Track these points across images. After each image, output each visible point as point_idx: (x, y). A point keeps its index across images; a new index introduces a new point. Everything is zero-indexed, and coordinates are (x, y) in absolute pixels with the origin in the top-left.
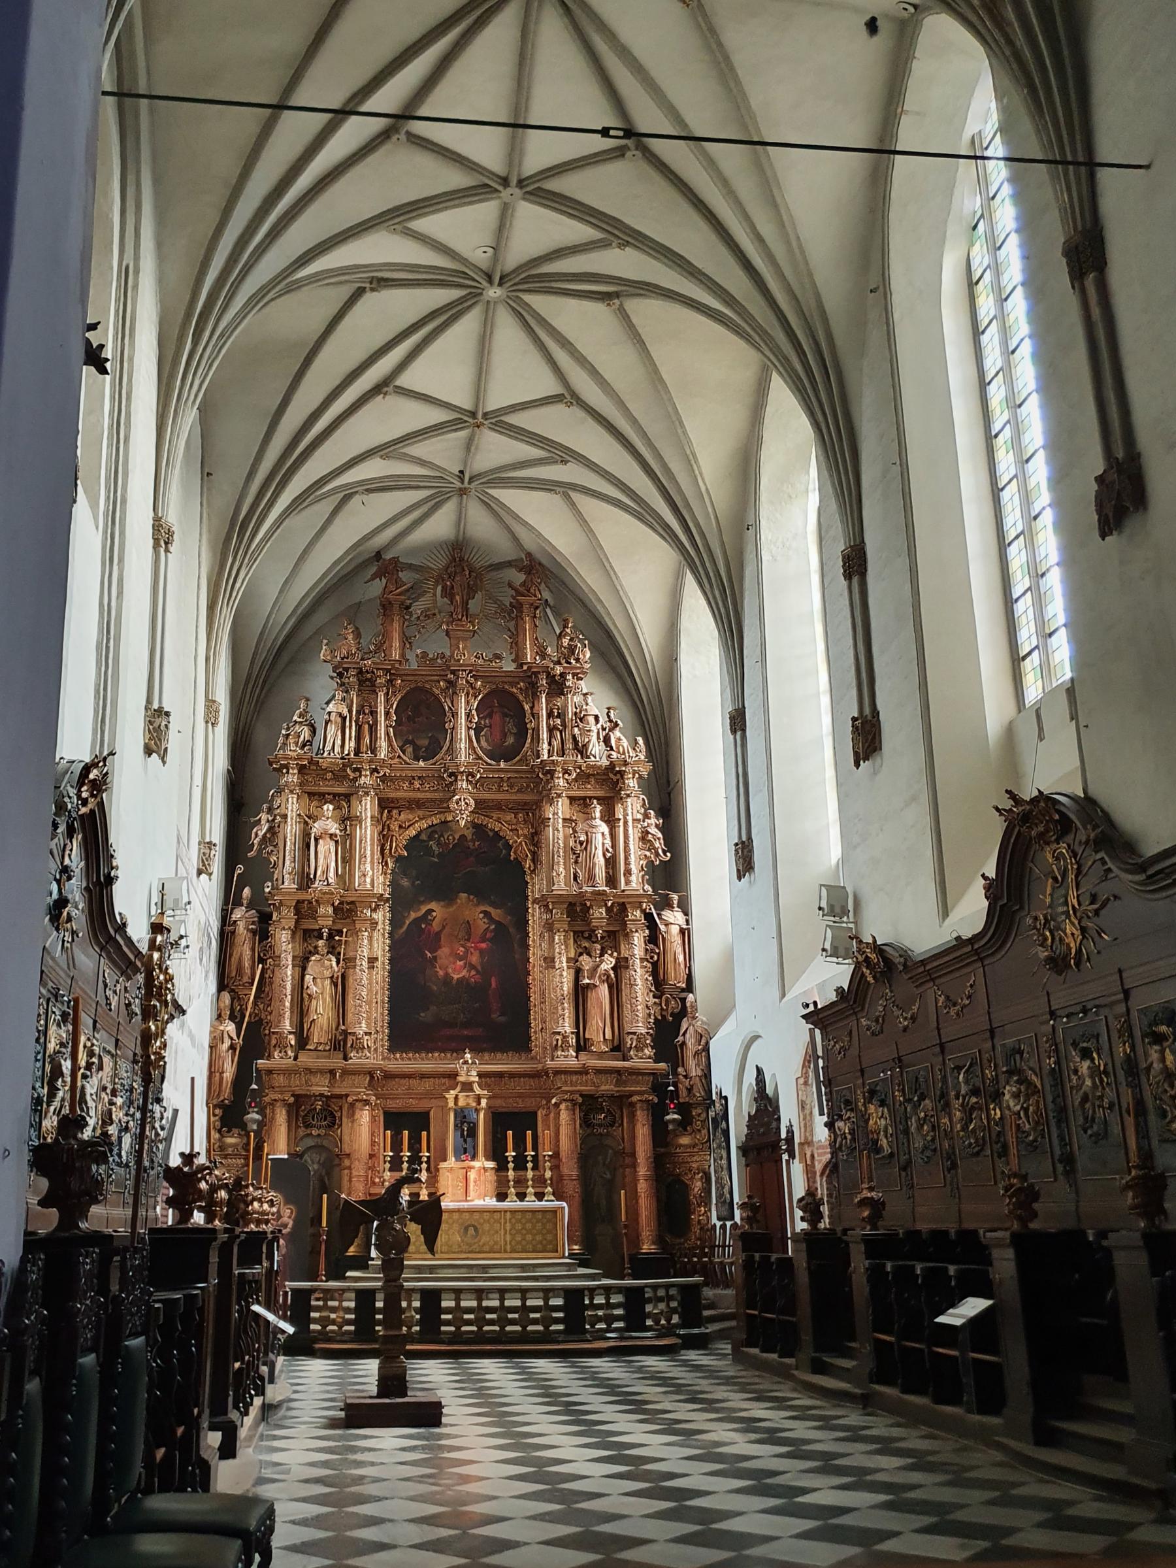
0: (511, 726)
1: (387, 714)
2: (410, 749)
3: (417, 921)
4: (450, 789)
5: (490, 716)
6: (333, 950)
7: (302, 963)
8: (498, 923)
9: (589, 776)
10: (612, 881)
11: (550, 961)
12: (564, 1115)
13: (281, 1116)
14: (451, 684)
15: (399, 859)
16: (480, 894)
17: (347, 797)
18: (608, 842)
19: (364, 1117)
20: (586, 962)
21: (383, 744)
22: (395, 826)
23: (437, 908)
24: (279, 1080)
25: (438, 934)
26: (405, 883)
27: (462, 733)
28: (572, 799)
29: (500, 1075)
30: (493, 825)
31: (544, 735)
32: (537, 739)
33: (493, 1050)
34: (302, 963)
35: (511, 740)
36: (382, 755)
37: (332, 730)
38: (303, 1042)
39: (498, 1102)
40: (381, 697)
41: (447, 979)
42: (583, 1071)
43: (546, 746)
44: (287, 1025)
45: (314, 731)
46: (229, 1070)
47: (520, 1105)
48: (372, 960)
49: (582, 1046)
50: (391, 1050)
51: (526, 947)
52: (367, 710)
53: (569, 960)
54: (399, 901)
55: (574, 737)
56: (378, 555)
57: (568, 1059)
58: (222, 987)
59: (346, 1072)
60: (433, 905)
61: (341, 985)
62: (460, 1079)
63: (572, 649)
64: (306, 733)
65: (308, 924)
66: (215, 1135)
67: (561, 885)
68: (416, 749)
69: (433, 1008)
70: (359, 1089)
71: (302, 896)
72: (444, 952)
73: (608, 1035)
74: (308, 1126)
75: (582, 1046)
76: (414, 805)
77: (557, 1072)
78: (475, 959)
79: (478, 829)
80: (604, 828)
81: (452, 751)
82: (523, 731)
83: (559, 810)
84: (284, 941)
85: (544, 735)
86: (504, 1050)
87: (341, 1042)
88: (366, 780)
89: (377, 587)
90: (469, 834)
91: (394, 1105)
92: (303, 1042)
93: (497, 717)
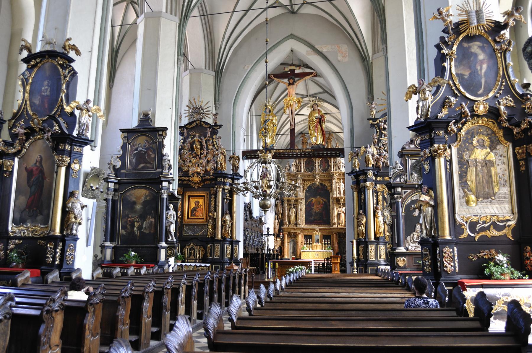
0: (326, 165)
1: (303, 164)
2: (308, 170)
3: (310, 202)
4: (314, 177)
5: (323, 163)
6: (294, 207)
7: (289, 210)
9: (340, 174)
11: (333, 209)
12: (335, 236)
13: (286, 236)
15: (306, 190)
16: (321, 196)
17: (296, 180)
19: (300, 236)
20: (340, 209)
21: (303, 170)
22: (305, 184)
23: (314, 199)
24: (286, 230)
25: (314, 204)
26: (308, 194)
27: (317, 167)
28: (338, 179)
29: (324, 229)
30: (324, 183)
31: (332, 166)
32: (331, 167)
33: (323, 224)
34: (289, 210)
35: (326, 167)
36: (302, 172)
37: (293, 167)
38: (290, 223)
39: (324, 234)
40: (302, 161)
41: (315, 212)
42: (338, 228)
43: (332, 169)
44: (287, 221)
45: (290, 168)
46: (277, 228)
47: (327, 234)
48: (301, 209)
49: (339, 224)
50: (306, 224)
51: (330, 206)
52: (300, 163)
53: (336, 209)
54: (307, 198)
55: (338, 167)
56: (302, 132)
57: (335, 226)
58: (276, 214)
59: (296, 229)
60: (313, 198)
61: (296, 213)
62: (316, 230)
64: (289, 168)
65: (290, 203)
66: (275, 239)
67: (335, 196)
68: (309, 170)
69: (313, 217)
70: (298, 232)
71: (289, 198)
72: (315, 207)
73: (343, 222)
74: (291, 237)
75: (339, 224)
76: (308, 180)
77: (333, 229)
78: (320, 208)
79: (321, 184)
81: (315, 170)
82: (329, 166)
83: (335, 181)
84: (286, 206)
85: (332, 166)
86: (325, 224)
87: (296, 224)
88: (299, 177)
89: (302, 138)
90: (319, 185)
91: (306, 234)
92: (290, 223)
93: (324, 163)
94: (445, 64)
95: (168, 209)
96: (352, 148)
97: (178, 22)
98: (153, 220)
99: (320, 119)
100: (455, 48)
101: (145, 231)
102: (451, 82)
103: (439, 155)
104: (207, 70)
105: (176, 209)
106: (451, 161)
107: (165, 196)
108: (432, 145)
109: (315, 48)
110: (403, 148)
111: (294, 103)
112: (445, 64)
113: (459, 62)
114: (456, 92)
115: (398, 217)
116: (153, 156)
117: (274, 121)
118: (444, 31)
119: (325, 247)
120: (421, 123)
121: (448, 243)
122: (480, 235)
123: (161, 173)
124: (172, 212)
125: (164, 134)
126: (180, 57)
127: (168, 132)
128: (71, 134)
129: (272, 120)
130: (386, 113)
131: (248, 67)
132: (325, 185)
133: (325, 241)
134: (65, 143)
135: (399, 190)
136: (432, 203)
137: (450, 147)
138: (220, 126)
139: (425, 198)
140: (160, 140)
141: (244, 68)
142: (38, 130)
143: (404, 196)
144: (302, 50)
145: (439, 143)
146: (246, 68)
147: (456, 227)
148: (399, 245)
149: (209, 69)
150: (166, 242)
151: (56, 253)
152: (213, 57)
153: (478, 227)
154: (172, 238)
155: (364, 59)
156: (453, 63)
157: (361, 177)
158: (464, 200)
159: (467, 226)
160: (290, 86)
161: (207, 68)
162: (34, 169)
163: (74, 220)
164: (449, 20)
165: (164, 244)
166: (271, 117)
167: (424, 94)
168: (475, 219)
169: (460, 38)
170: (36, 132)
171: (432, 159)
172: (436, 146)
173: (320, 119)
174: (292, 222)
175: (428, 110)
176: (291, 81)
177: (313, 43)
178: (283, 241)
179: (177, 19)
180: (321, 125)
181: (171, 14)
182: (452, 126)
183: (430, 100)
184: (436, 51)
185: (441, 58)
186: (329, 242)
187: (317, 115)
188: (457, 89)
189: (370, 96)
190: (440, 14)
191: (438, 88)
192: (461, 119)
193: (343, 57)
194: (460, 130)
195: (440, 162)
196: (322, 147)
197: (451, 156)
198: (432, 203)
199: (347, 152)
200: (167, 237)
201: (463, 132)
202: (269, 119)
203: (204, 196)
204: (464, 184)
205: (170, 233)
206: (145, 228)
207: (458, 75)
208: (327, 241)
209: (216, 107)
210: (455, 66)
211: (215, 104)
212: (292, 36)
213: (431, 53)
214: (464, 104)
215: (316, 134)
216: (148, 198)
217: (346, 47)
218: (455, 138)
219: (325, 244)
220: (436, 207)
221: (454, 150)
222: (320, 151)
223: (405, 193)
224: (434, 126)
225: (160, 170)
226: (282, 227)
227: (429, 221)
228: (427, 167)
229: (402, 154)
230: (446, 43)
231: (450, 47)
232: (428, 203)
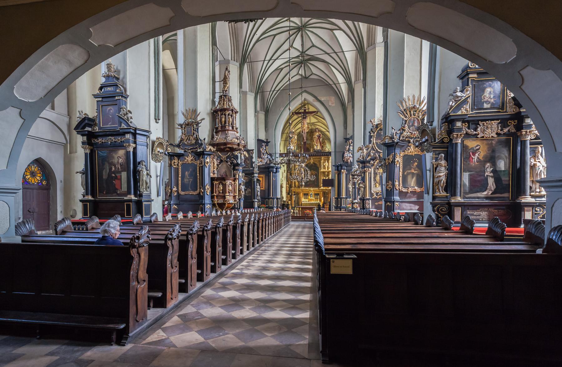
8: (316, 174)
10: (328, 169)
14: (311, 147)
18: (328, 165)
19: (301, 194)
28: (324, 160)
30: (315, 162)
38: (295, 186)
44: (293, 185)
46: (288, 189)
58: (287, 181)
63: (324, 142)
67: (322, 170)
79: (314, 163)
80: (327, 163)
83: (322, 161)
94: (372, 139)
95: (257, 185)
96: (335, 152)
97: (254, 96)
98: (250, 190)
99: (319, 137)
100: (376, 133)
101: (247, 195)
102: (373, 145)
103: (367, 172)
104: (261, 112)
105: (260, 185)
106: (371, 173)
107: (256, 180)
108: (365, 168)
109: (317, 98)
110: (358, 159)
111: (306, 129)
112: (372, 139)
113: (377, 139)
114: (375, 149)
115: (355, 188)
116: (248, 162)
117: (295, 138)
118: (372, 127)
119: (316, 200)
120: (362, 161)
121: (369, 199)
122: (379, 196)
123: (253, 170)
124: (258, 187)
125: (253, 152)
126: (256, 114)
127: (254, 151)
128: (237, 163)
129: (294, 137)
130: (352, 136)
131: (282, 109)
132: (316, 164)
133: (316, 197)
134: (237, 166)
135: (356, 177)
136: (364, 187)
137: (371, 168)
138: (270, 142)
139: (361, 185)
140: (251, 155)
141: (280, 109)
142: (224, 161)
143: (358, 179)
144: (310, 99)
145: (367, 168)
146: (281, 109)
147: (372, 195)
148: (355, 199)
149: (262, 111)
150: (257, 199)
151: (238, 204)
152: (264, 104)
153: (379, 194)
154: (259, 198)
155: (343, 104)
156: (375, 139)
157: (340, 168)
158: (375, 186)
159: (375, 194)
160: (304, 119)
161: (261, 110)
162: (223, 175)
163: (242, 193)
164: (374, 123)
165: (256, 200)
166: (294, 136)
167: (363, 151)
168: (378, 192)
169: (378, 129)
170: (223, 161)
171: (364, 173)
172: (366, 169)
173: (319, 137)
174: (297, 186)
175: (364, 156)
176: (305, 117)
177: (316, 95)
178: (291, 196)
179: (254, 94)
180: (319, 139)
181: (251, 92)
182: (372, 162)
183: (365, 153)
184: (369, 134)
185: (371, 137)
186: (319, 197)
187: (318, 134)
188: (375, 148)
189: (345, 125)
190: (371, 122)
191: (368, 148)
192: (375, 159)
193: (332, 103)
194: (375, 162)
195: (367, 174)
196: (320, 151)
197: (371, 171)
198: (364, 187)
199: (333, 154)
200: (257, 197)
201: (376, 163)
202: (293, 137)
203: (263, 177)
204: (375, 180)
205: (258, 195)
206: (247, 194)
207: (375, 143)
208: (318, 197)
209: (266, 131)
210: (375, 140)
211: (265, 129)
212: (306, 91)
213: (368, 134)
214: (376, 154)
215: (317, 144)
216: (247, 181)
217: (334, 98)
218: (373, 165)
219: (316, 198)
220: (365, 188)
221: (372, 169)
222: (319, 153)
223: (358, 178)
224: (365, 162)
225: (252, 169)
226: (291, 189)
227: (362, 193)
228: (363, 175)
229: (358, 162)
230: (373, 131)
231: (374, 133)
232: (362, 187)
